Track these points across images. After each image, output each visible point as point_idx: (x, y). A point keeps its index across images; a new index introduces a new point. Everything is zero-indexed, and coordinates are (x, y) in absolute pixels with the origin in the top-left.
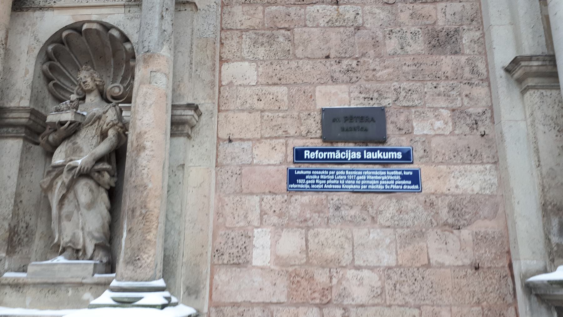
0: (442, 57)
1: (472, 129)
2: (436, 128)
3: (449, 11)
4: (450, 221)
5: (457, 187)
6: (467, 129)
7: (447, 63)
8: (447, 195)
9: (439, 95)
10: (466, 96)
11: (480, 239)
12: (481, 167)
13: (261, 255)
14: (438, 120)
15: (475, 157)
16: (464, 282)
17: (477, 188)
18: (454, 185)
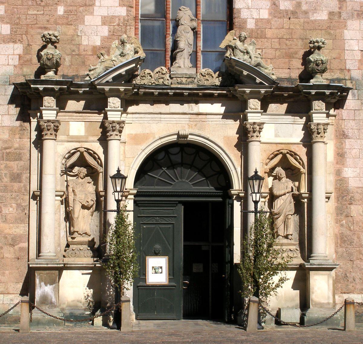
0: (15, 184)
1: (22, 211)
2: (10, 211)
3: (19, 166)
4: (12, 243)
5: (15, 232)
6: (20, 211)
7: (16, 186)
8: (11, 235)
9: (12, 198)
10: (22, 199)
11: (21, 249)
12: (24, 225)
14: (11, 208)
15: (22, 221)
16: (14, 263)
17: (21, 232)
18: (14, 231)
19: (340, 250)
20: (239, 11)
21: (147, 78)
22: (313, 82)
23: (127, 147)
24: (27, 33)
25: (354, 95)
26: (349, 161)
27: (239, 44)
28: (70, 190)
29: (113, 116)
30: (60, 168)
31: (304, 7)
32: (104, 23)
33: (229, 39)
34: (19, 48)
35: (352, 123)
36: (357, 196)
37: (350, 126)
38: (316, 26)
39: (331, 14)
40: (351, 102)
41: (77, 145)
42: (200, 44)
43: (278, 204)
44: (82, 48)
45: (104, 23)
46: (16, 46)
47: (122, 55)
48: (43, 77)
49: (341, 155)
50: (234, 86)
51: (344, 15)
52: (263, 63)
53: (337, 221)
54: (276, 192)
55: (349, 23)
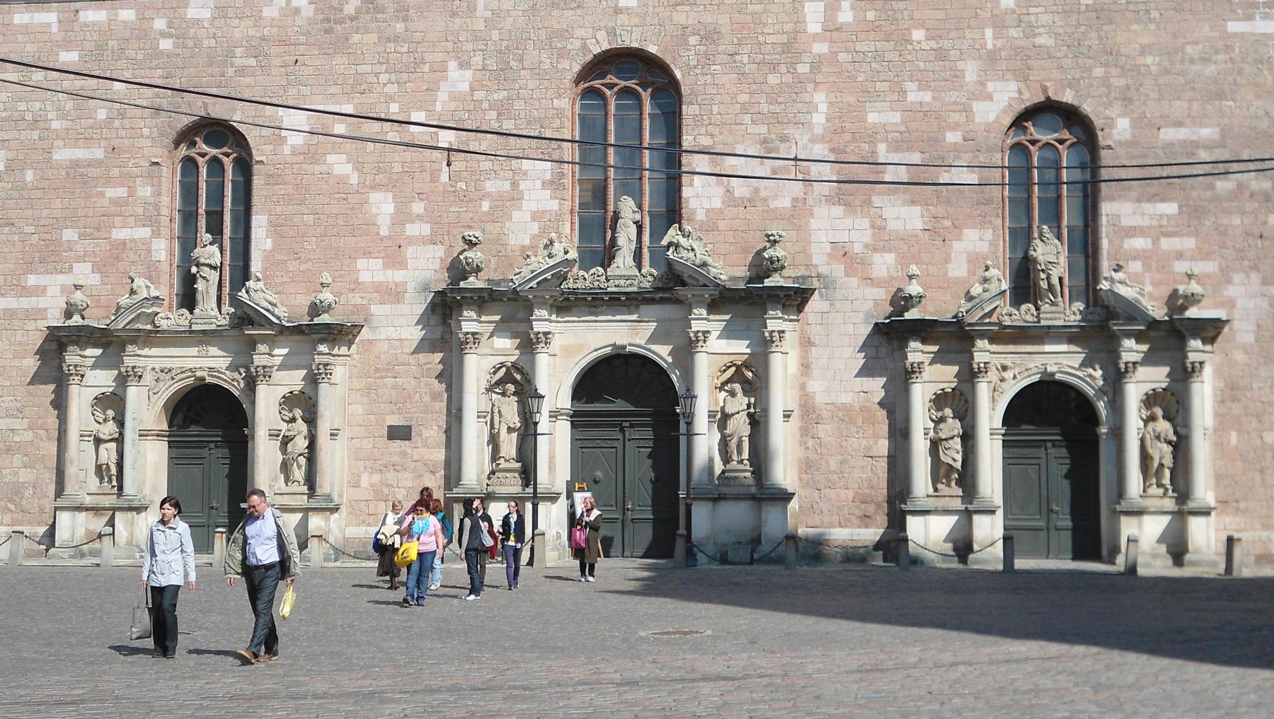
13: (364, 483)
19: (805, 477)
20: (687, 200)
21: (583, 279)
22: (768, 282)
23: (557, 360)
24: (448, 233)
25: (821, 295)
26: (816, 372)
27: (683, 241)
28: (496, 410)
29: (538, 327)
30: (484, 384)
31: (763, 194)
32: (533, 219)
33: (672, 234)
34: (439, 251)
35: (819, 328)
36: (825, 414)
37: (815, 331)
38: (777, 215)
39: (795, 200)
40: (814, 304)
41: (502, 359)
42: (646, 238)
43: (732, 425)
44: (509, 248)
45: (533, 219)
46: (437, 247)
47: (550, 256)
48: (462, 284)
49: (806, 367)
50: (673, 287)
51: (810, 201)
52: (709, 260)
53: (803, 444)
54: (729, 410)
55: (816, 210)
